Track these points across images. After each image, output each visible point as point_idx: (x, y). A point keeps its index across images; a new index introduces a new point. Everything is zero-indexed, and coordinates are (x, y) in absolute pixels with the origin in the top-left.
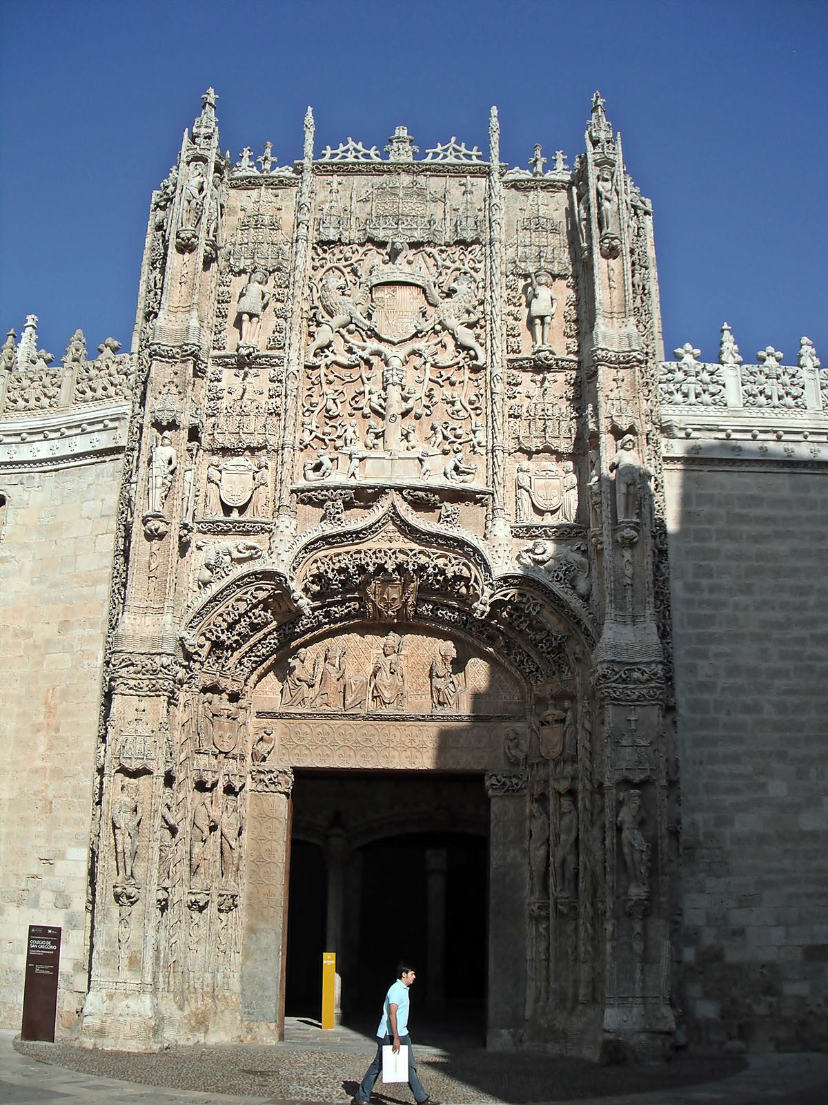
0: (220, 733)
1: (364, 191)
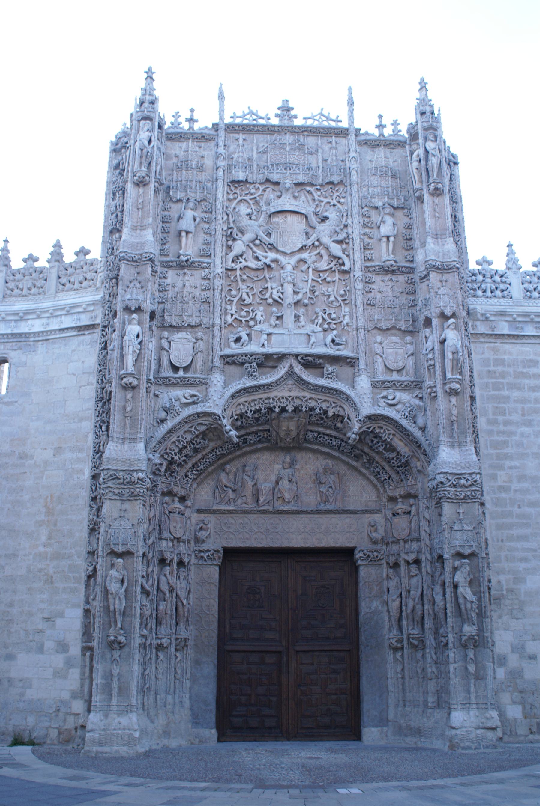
1: (261, 145)
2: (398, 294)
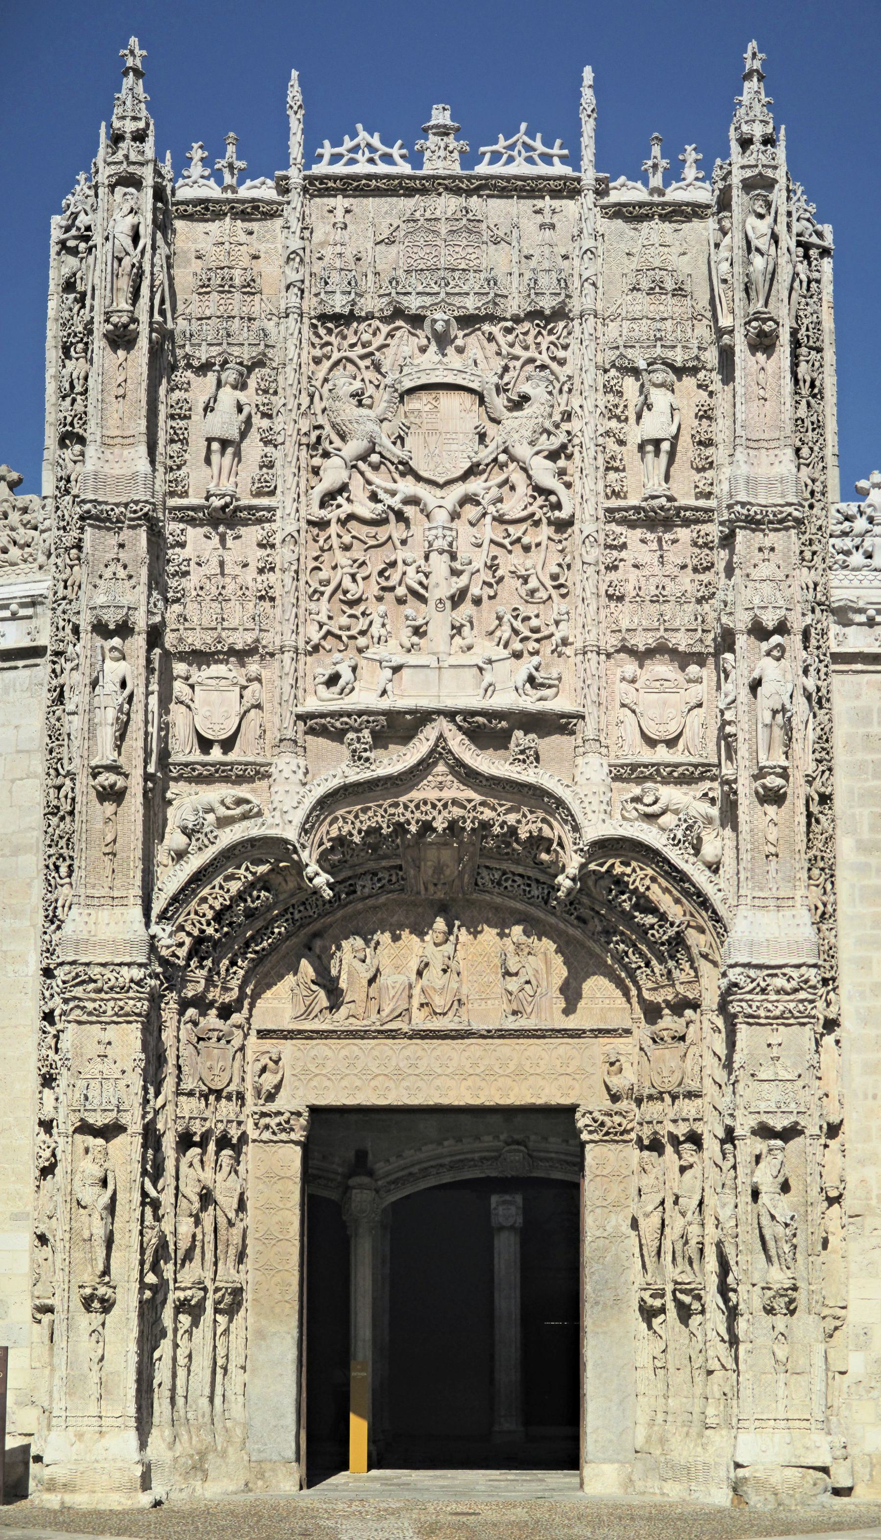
0: (208, 1064)
2: (676, 571)
